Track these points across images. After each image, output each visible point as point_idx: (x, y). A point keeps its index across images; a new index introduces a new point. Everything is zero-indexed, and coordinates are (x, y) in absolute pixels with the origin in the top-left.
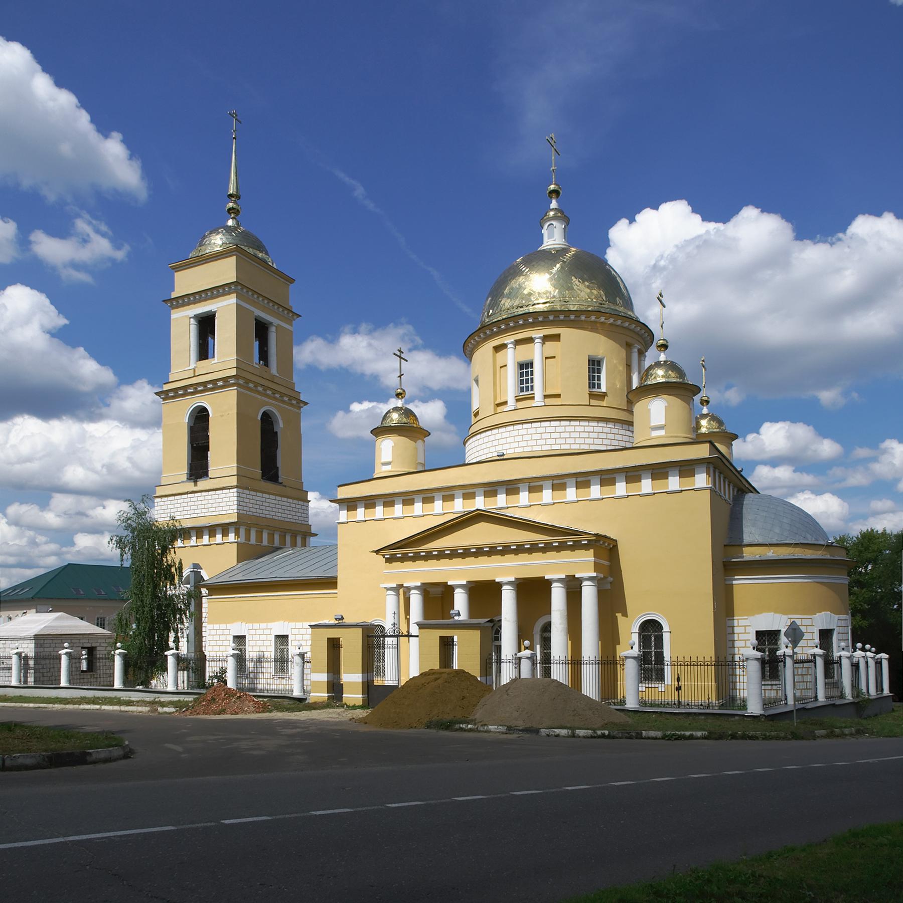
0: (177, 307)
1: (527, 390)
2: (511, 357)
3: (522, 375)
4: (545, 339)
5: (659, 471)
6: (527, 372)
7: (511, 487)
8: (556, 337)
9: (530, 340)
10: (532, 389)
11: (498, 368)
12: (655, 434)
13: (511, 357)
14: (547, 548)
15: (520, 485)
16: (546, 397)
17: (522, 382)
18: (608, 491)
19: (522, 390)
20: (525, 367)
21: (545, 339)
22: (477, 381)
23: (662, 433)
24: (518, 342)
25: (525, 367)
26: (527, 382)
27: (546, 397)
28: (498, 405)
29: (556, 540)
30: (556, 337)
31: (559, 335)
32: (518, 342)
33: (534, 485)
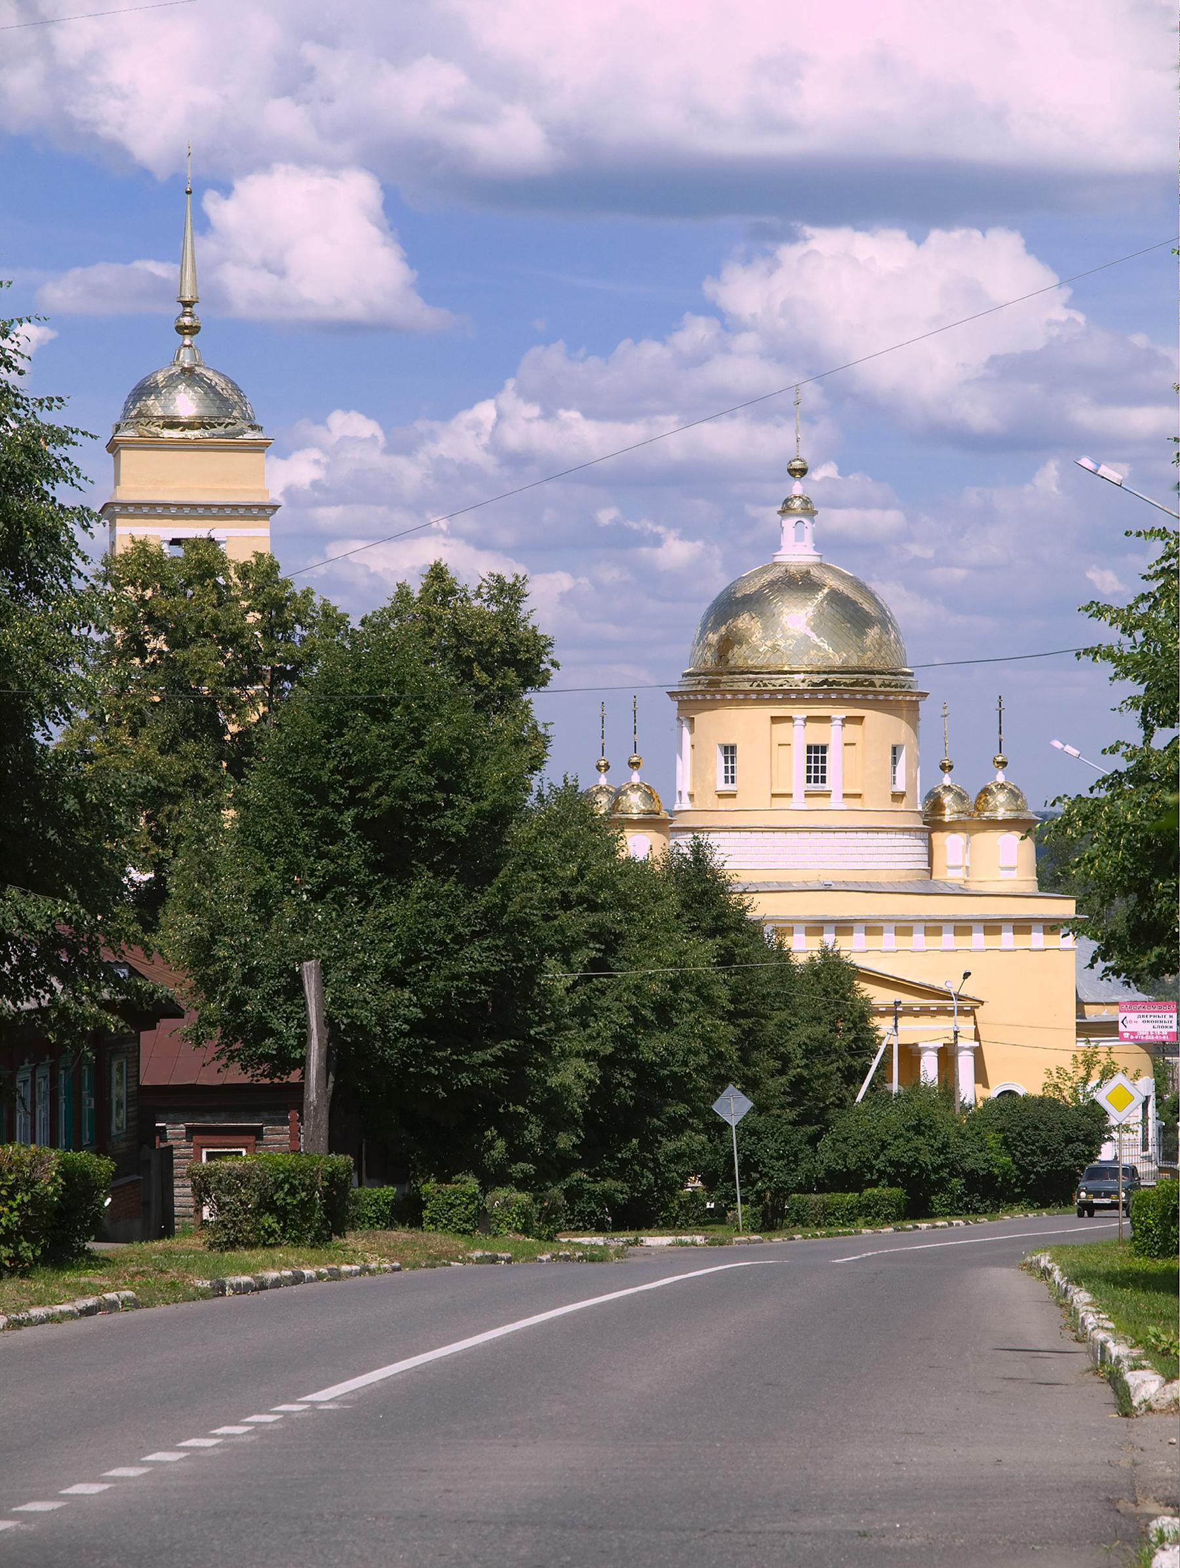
0: (132, 516)
1: (816, 781)
2: (800, 735)
3: (809, 760)
4: (848, 720)
5: (1022, 926)
6: (816, 759)
7: (843, 927)
8: (859, 720)
9: (827, 719)
10: (824, 780)
11: (775, 746)
12: (1004, 875)
13: (800, 735)
14: (924, 1012)
15: (856, 926)
16: (845, 796)
17: (809, 769)
18: (962, 942)
19: (809, 780)
20: (817, 753)
21: (848, 720)
22: (729, 751)
23: (1014, 875)
24: (809, 719)
25: (817, 753)
26: (816, 770)
27: (845, 796)
28: (773, 795)
29: (934, 1003)
30: (859, 720)
31: (862, 718)
32: (809, 719)
33: (873, 927)
